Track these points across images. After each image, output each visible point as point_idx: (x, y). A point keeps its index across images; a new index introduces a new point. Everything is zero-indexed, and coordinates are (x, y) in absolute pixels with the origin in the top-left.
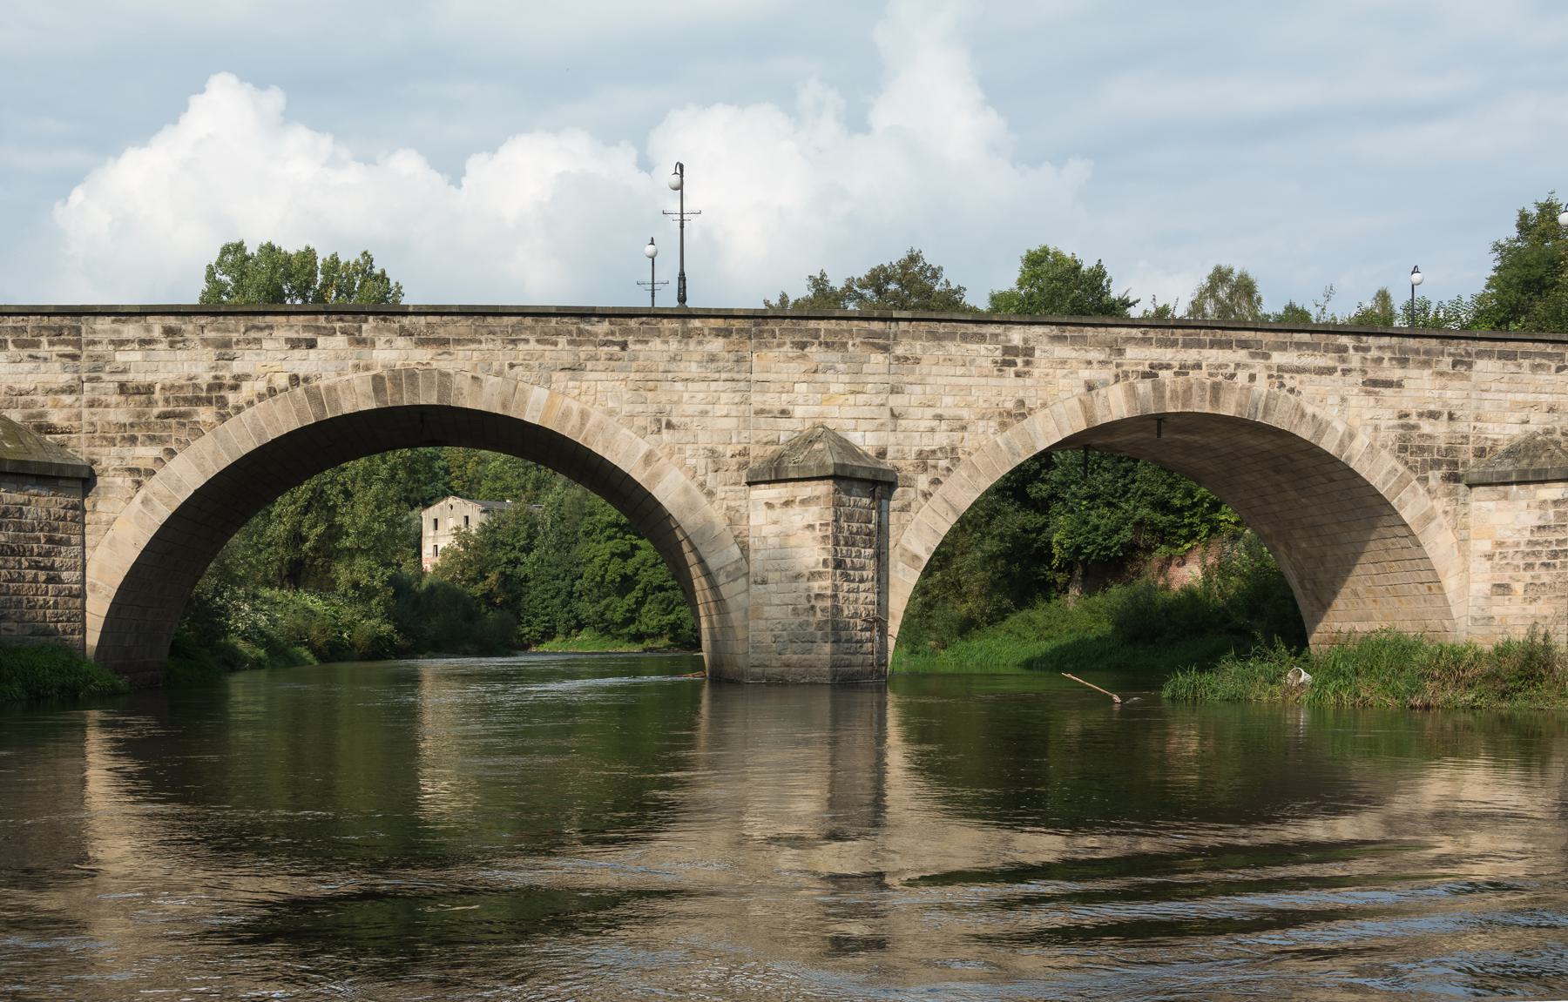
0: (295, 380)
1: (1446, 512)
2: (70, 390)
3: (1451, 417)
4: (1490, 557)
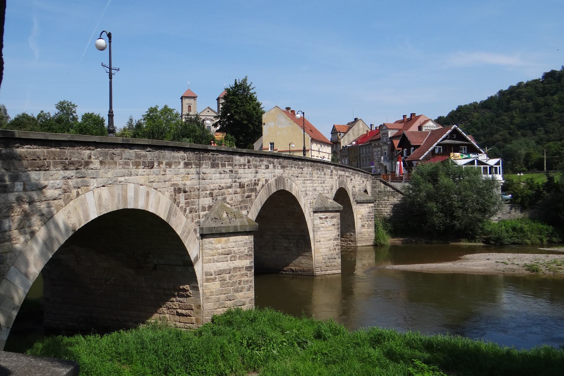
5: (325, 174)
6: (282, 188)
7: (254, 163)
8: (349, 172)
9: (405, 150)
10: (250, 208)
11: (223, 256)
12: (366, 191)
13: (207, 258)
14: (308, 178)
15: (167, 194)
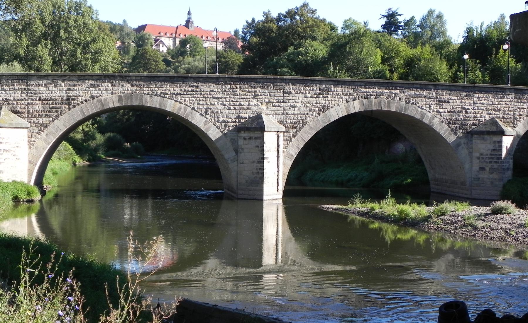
0: (93, 97)
1: (464, 143)
3: (466, 112)
4: (479, 158)
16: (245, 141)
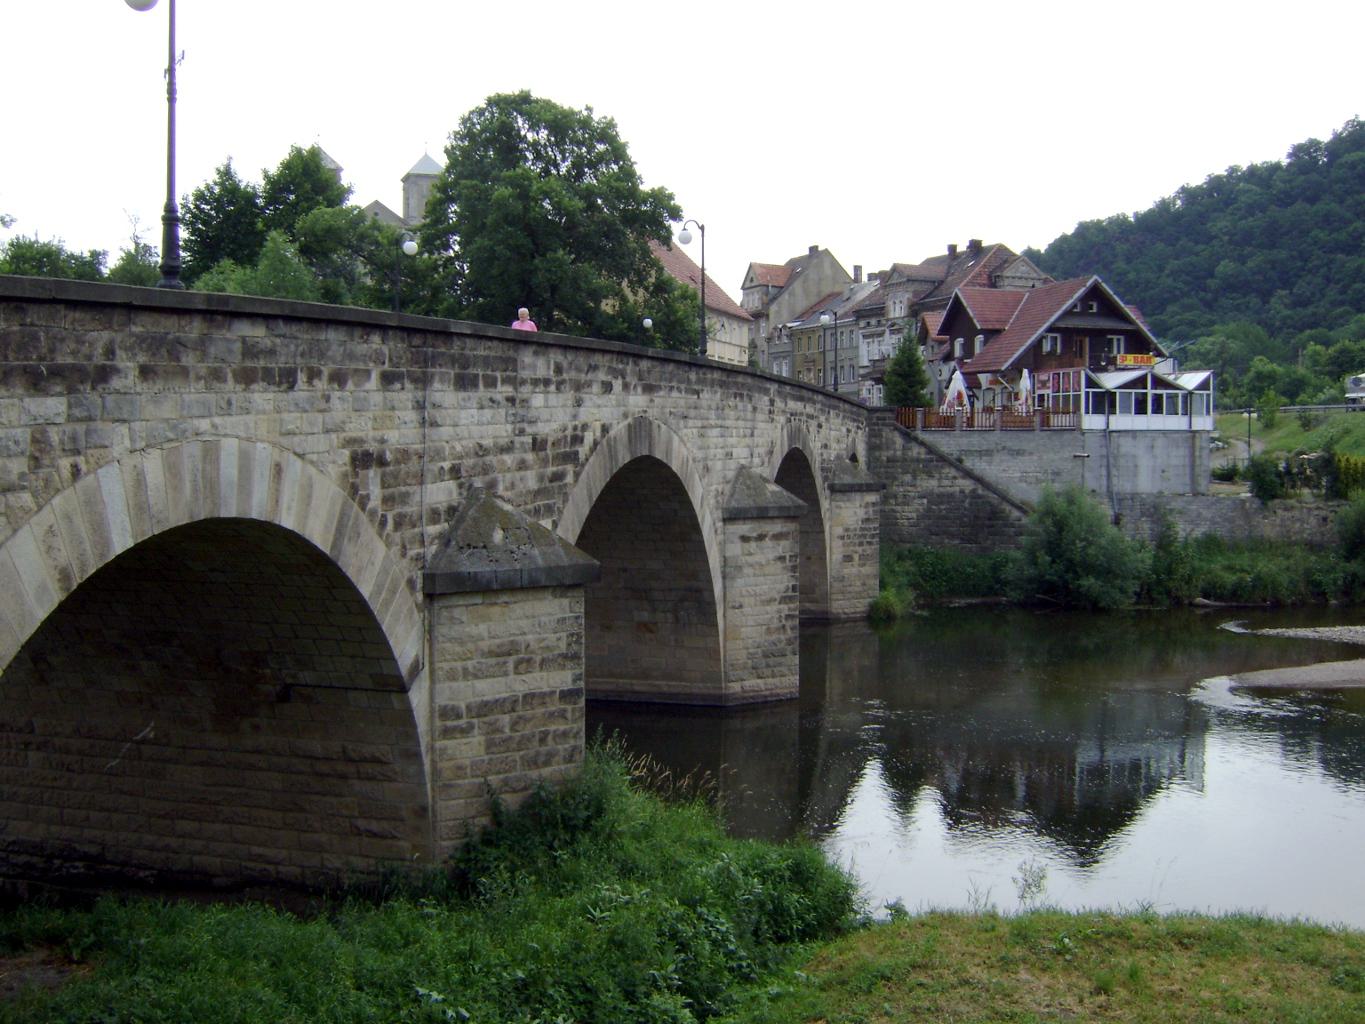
2: (508, 449)
4: (842, 538)
5: (755, 409)
6: (645, 452)
7: (573, 374)
8: (814, 403)
9: (959, 341)
10: (560, 512)
11: (493, 661)
12: (854, 458)
13: (446, 666)
14: (712, 422)
15: (334, 471)
16: (746, 545)
